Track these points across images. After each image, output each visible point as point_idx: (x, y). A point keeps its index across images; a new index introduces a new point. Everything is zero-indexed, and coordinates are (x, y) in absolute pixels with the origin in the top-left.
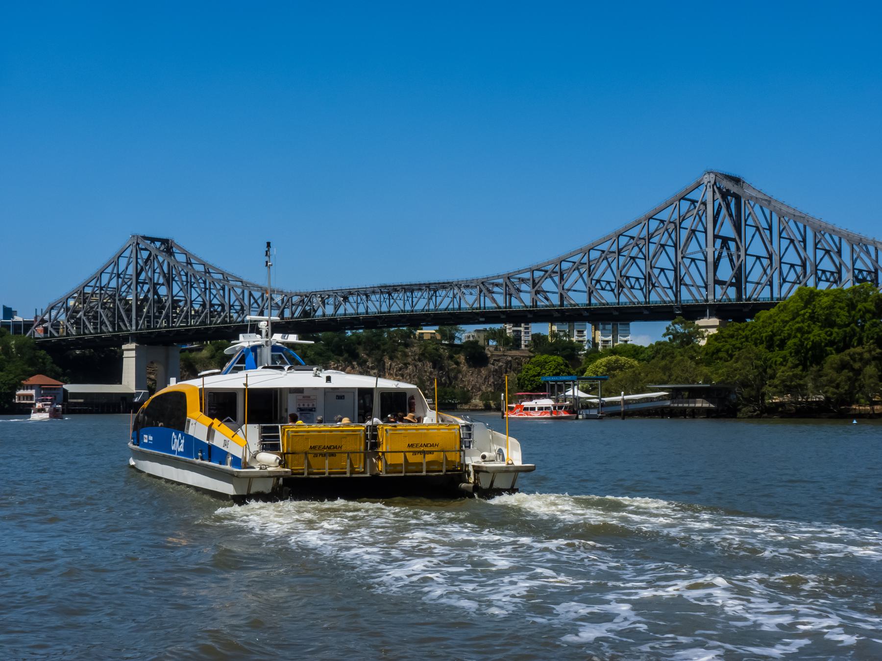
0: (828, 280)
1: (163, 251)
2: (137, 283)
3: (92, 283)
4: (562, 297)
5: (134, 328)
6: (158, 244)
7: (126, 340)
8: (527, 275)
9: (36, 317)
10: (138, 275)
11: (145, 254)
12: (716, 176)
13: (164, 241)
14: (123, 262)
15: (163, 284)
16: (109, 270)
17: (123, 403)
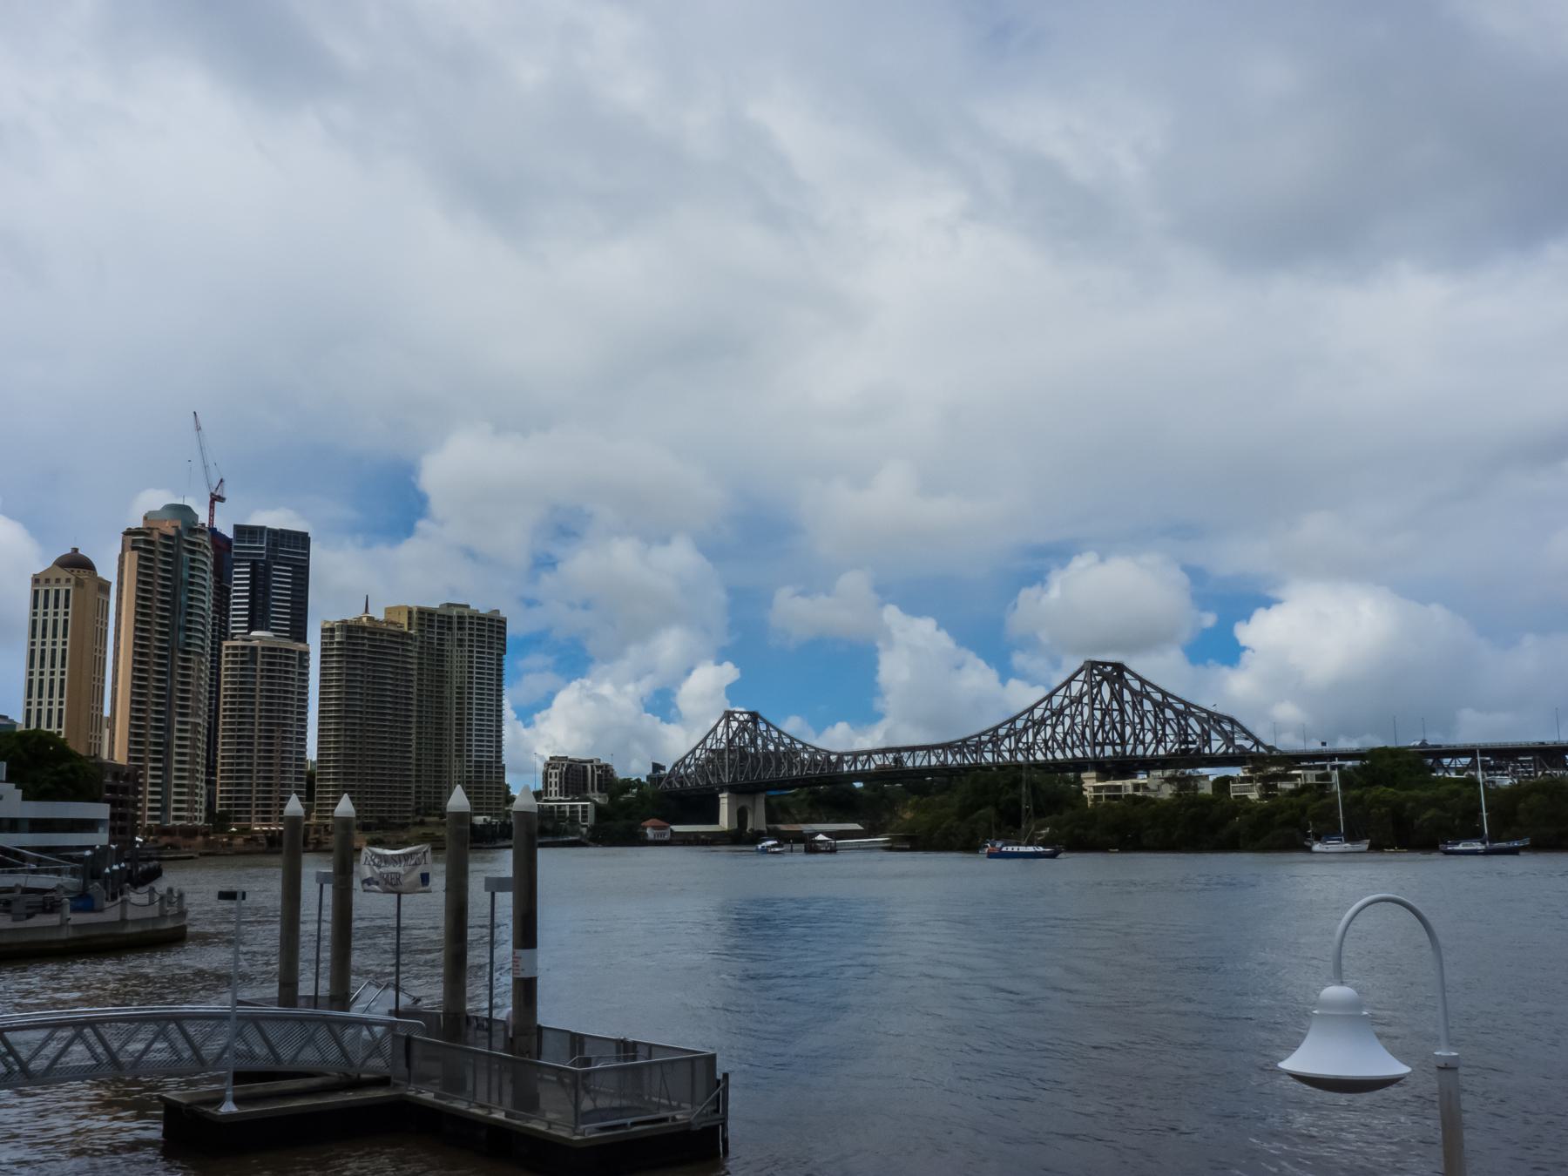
0: (1171, 741)
3: (700, 747)
4: (1011, 756)
7: (722, 792)
8: (977, 739)
10: (730, 741)
11: (734, 725)
14: (720, 730)
16: (711, 736)
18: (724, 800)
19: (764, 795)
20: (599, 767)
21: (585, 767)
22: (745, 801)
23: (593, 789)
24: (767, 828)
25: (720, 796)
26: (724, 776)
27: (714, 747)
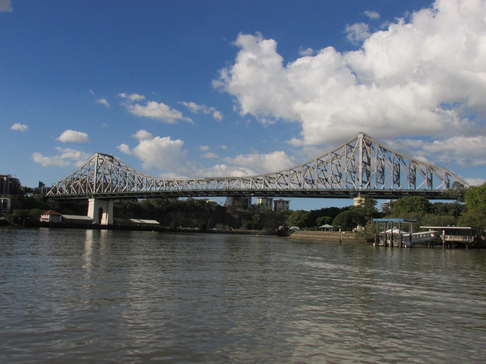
1: (108, 160)
2: (97, 173)
5: (94, 192)
6: (107, 157)
7: (91, 198)
9: (52, 187)
10: (97, 170)
11: (101, 161)
12: (364, 135)
13: (109, 156)
15: (108, 175)
17: (88, 225)
18: (92, 203)
19: (113, 202)
20: (12, 180)
21: (3, 179)
22: (103, 205)
23: (6, 191)
24: (113, 220)
25: (89, 200)
26: (93, 189)
27: (87, 173)
